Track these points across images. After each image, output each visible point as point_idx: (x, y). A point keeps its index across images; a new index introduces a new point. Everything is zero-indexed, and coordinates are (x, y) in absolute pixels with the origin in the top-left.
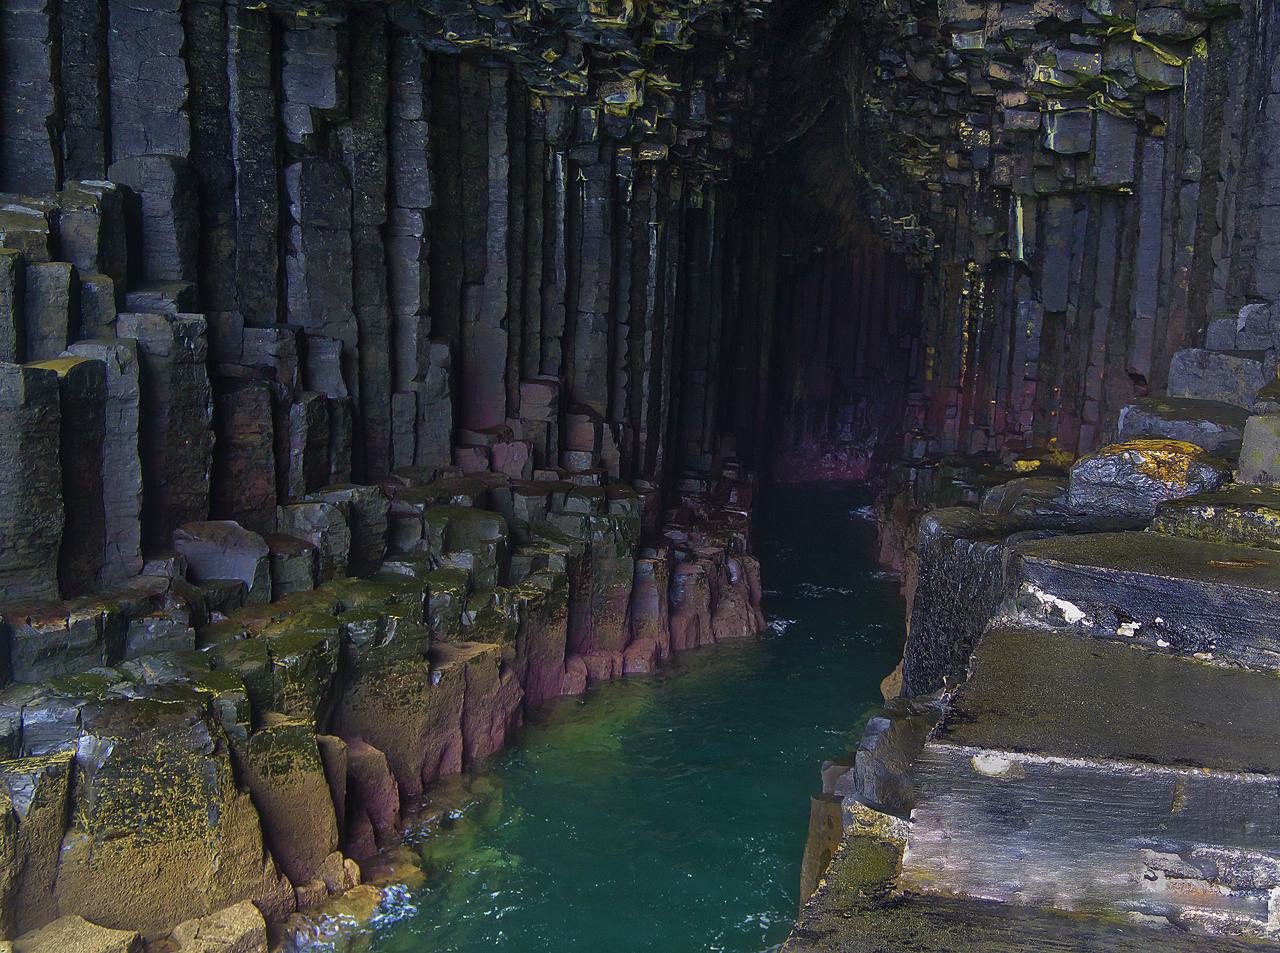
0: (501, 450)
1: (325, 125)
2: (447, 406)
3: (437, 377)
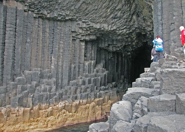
0: (121, 80)
1: (111, 58)
2: (117, 77)
3: (117, 75)
